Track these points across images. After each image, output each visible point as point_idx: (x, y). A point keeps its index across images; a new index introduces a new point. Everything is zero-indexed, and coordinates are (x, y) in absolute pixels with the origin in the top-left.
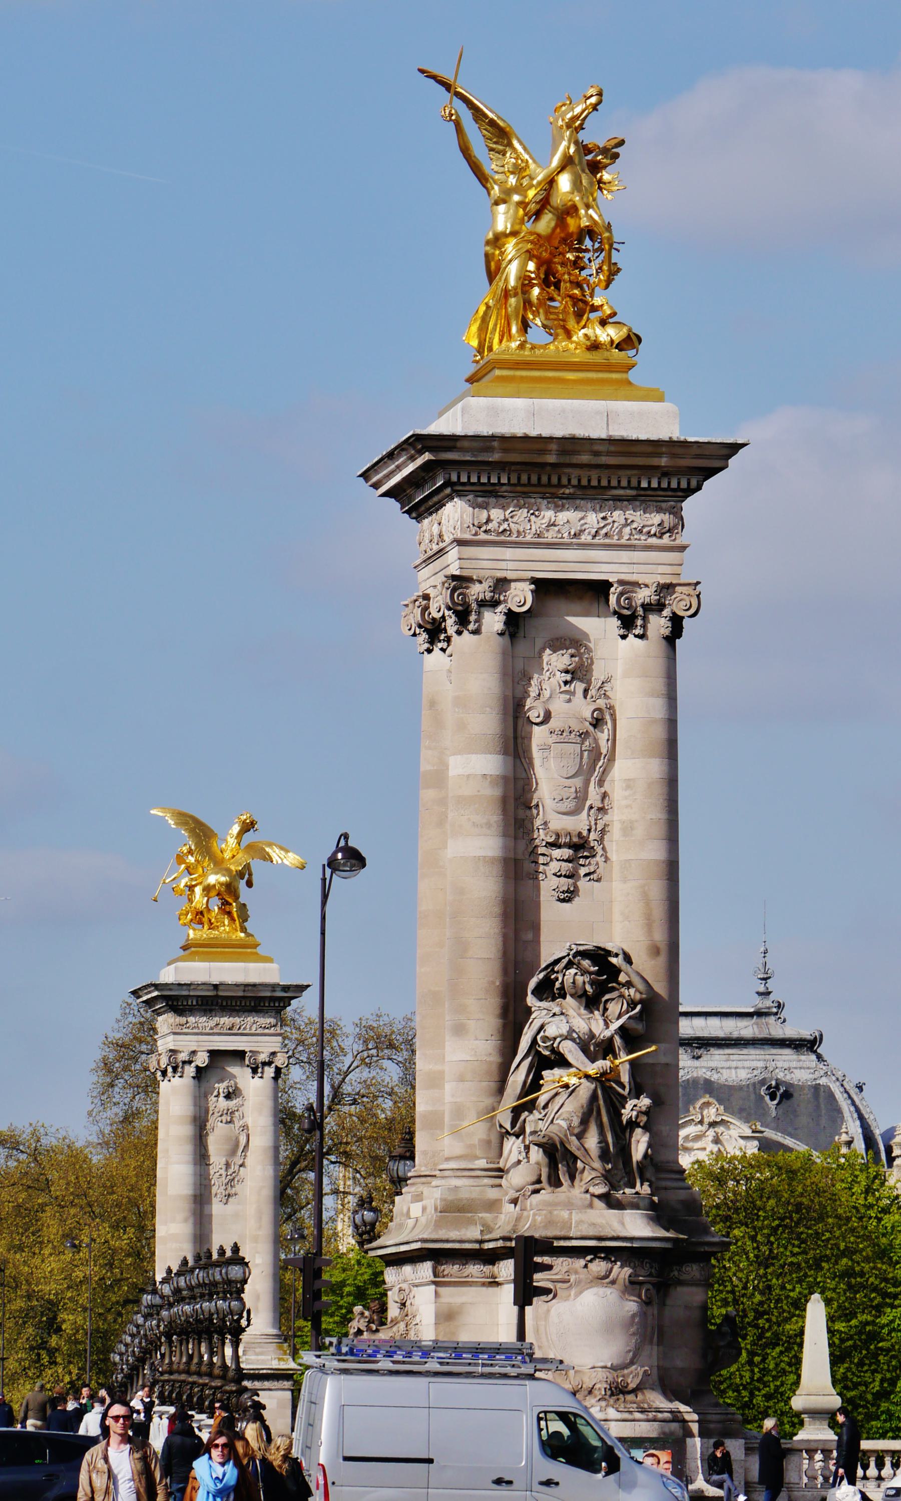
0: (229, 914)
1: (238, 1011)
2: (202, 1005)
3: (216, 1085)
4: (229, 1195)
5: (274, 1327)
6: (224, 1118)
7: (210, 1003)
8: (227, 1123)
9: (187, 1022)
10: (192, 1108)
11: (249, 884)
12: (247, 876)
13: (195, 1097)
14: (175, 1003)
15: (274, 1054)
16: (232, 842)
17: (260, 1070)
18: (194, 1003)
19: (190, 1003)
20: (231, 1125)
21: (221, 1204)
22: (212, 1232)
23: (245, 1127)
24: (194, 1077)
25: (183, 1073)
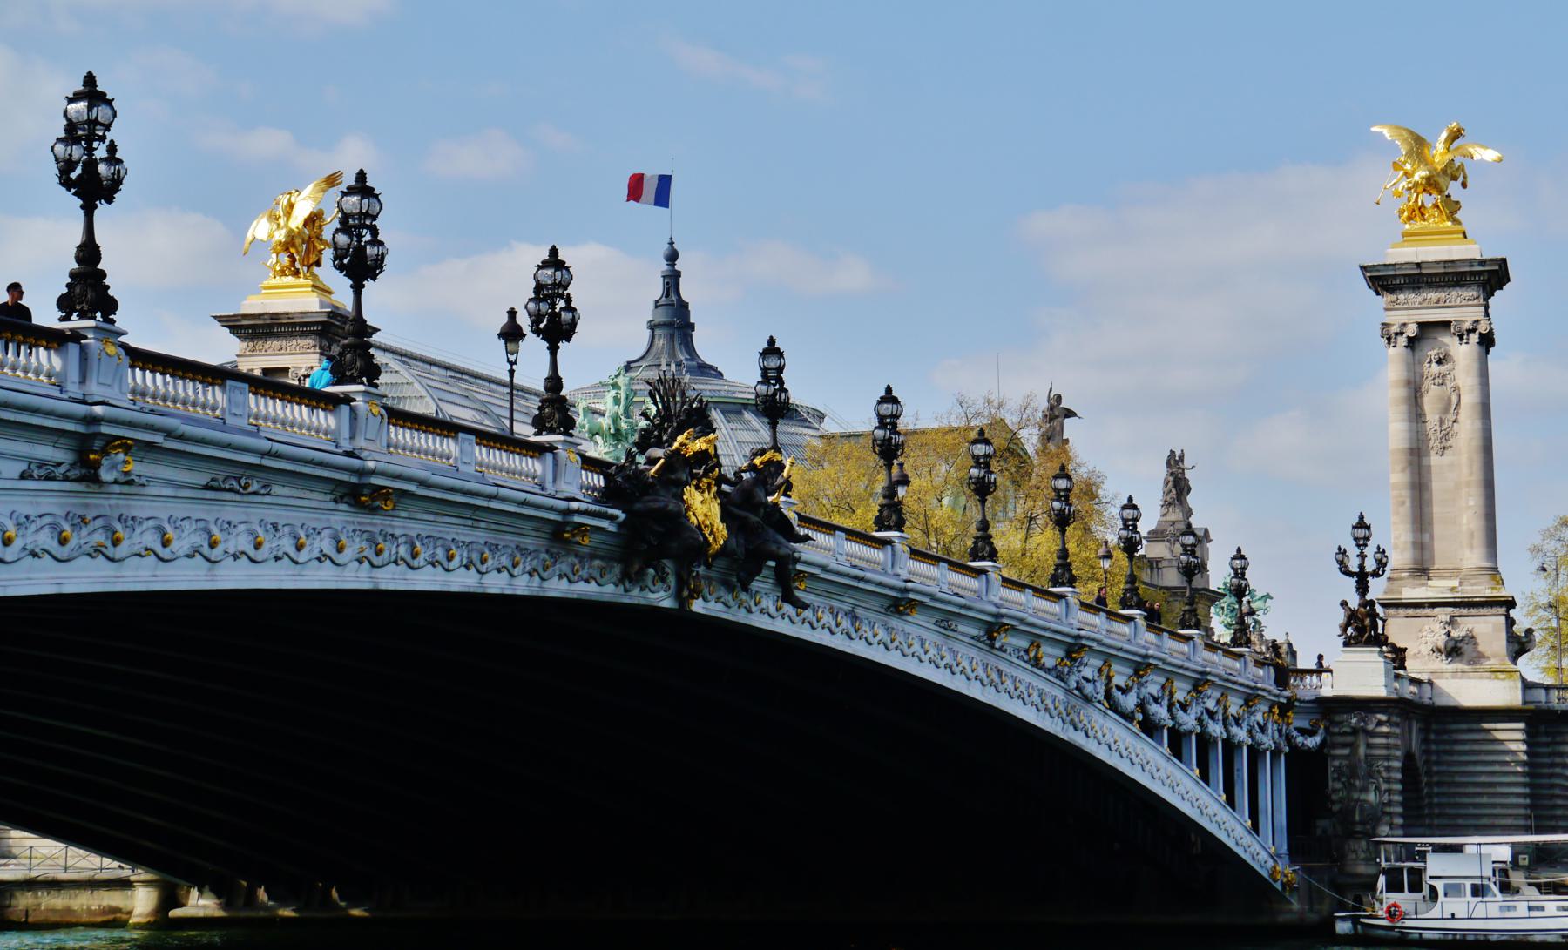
0: (1438, 207)
1: (1443, 287)
2: (1409, 283)
3: (1429, 353)
4: (1444, 448)
5: (1488, 561)
6: (1436, 381)
7: (1416, 280)
8: (1439, 385)
9: (1398, 299)
10: (1405, 373)
11: (1464, 185)
12: (1461, 179)
13: (1408, 364)
14: (1385, 283)
15: (1477, 322)
16: (1440, 147)
17: (1465, 337)
18: (1402, 282)
19: (1398, 282)
20: (1444, 387)
21: (1438, 457)
22: (1431, 481)
23: (1456, 389)
24: (1406, 347)
25: (1396, 343)
